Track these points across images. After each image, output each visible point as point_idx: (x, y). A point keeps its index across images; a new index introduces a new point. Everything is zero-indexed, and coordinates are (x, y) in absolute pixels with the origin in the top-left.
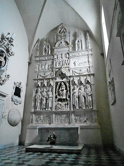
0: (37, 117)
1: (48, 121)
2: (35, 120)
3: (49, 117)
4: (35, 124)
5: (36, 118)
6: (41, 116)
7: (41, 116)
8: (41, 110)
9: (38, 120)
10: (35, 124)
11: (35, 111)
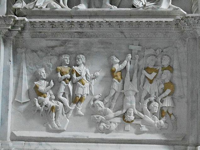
0: (37, 78)
1: (162, 113)
2: (17, 104)
3: (166, 75)
4: (15, 138)
5: (25, 85)
6: (83, 69)
7: (83, 69)
8: (82, 7)
9: (47, 101)
10: (15, 138)
11: (17, 12)
